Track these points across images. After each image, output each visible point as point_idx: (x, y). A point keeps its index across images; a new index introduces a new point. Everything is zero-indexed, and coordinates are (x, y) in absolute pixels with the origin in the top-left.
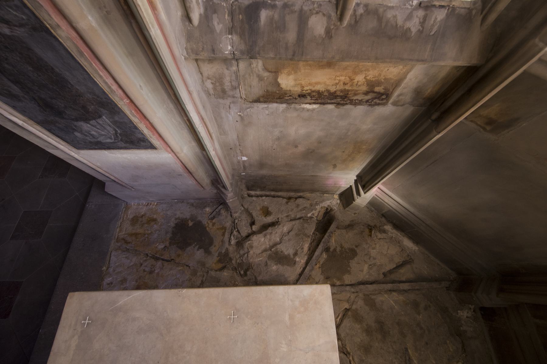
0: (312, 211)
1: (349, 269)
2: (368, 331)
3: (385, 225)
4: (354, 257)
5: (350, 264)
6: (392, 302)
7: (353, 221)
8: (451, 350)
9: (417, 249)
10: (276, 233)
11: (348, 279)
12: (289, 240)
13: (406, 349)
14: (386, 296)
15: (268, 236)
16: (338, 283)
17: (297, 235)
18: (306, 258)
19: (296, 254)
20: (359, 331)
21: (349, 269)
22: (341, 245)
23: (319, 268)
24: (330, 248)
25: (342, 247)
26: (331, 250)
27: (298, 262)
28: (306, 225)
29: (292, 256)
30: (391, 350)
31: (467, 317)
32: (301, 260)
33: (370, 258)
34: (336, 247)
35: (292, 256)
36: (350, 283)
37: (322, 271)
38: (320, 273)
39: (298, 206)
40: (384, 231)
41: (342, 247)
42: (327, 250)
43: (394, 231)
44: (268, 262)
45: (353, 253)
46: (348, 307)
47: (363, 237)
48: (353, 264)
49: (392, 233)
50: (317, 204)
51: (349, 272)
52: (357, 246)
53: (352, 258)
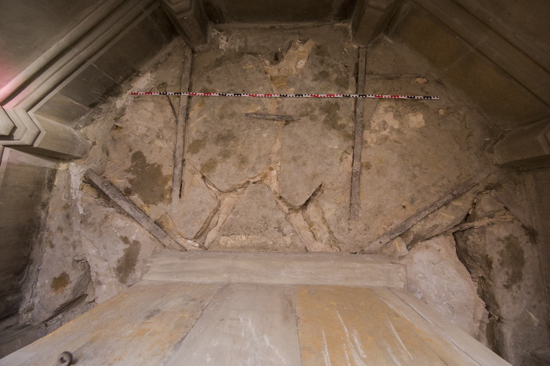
0: (76, 205)
1: (156, 166)
2: (226, 155)
3: (115, 106)
4: (143, 156)
5: (151, 163)
6: (199, 120)
7: (103, 149)
8: (252, 66)
9: (149, 74)
10: (96, 265)
11: (167, 171)
12: (105, 247)
13: (247, 115)
14: (192, 125)
15: (101, 278)
16: (170, 183)
17: (101, 235)
18: (135, 224)
19: (125, 240)
20: (224, 166)
21: (156, 166)
22: (126, 170)
23: (148, 206)
24: (127, 188)
25: (128, 171)
26: (130, 186)
27: (136, 237)
28: (90, 220)
29: (127, 246)
30: (246, 132)
31: (227, 41)
32: (138, 232)
33: (147, 136)
34: (127, 178)
35: (127, 246)
36: (172, 168)
37: (153, 204)
38: (153, 206)
39: (60, 229)
40: (123, 109)
41: (128, 171)
42: (128, 192)
43: (124, 96)
44: (129, 284)
45: (138, 157)
46: (201, 176)
47: (120, 138)
48: (151, 158)
49: (127, 101)
50: (69, 197)
51: (160, 167)
52: (131, 150)
53: (143, 159)
